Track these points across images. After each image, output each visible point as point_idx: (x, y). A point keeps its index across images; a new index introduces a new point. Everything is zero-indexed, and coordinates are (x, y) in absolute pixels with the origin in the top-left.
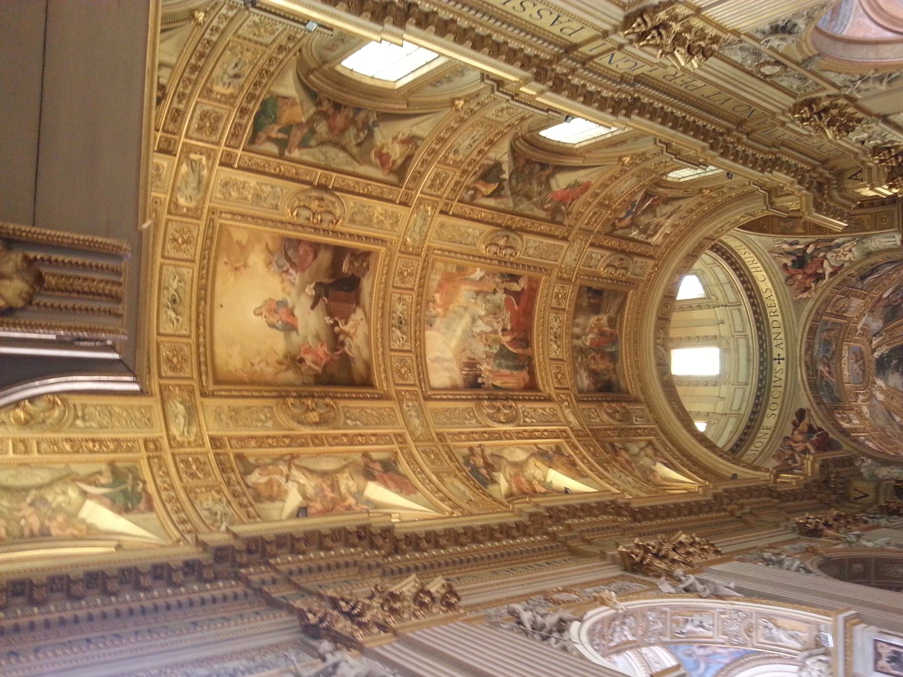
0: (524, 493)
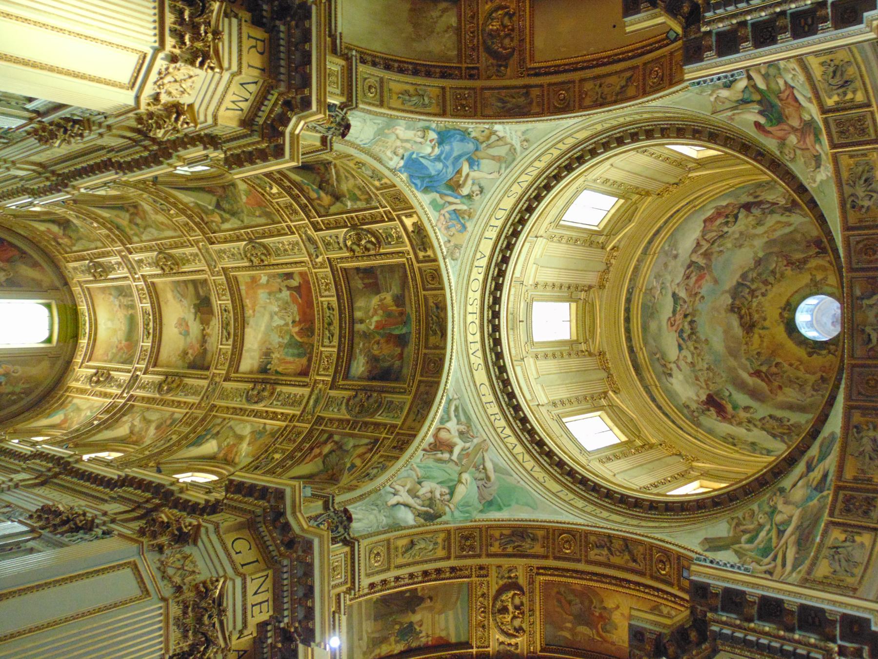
0: (226, 460)
